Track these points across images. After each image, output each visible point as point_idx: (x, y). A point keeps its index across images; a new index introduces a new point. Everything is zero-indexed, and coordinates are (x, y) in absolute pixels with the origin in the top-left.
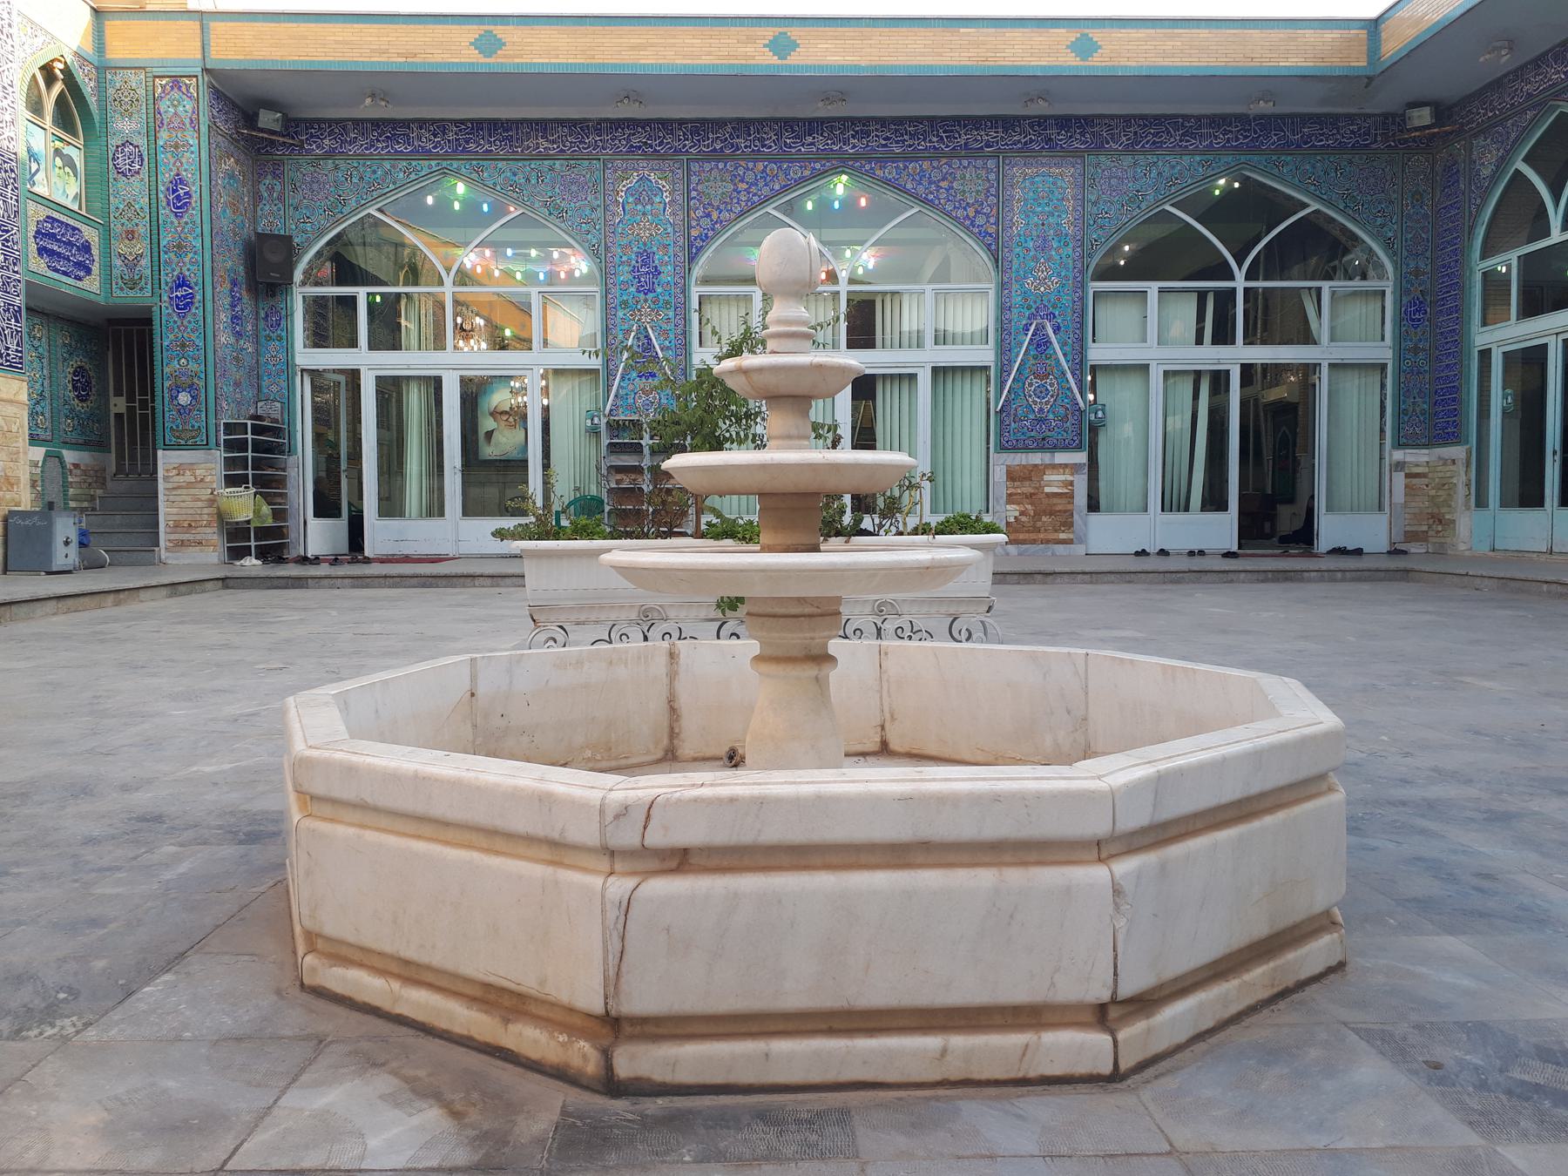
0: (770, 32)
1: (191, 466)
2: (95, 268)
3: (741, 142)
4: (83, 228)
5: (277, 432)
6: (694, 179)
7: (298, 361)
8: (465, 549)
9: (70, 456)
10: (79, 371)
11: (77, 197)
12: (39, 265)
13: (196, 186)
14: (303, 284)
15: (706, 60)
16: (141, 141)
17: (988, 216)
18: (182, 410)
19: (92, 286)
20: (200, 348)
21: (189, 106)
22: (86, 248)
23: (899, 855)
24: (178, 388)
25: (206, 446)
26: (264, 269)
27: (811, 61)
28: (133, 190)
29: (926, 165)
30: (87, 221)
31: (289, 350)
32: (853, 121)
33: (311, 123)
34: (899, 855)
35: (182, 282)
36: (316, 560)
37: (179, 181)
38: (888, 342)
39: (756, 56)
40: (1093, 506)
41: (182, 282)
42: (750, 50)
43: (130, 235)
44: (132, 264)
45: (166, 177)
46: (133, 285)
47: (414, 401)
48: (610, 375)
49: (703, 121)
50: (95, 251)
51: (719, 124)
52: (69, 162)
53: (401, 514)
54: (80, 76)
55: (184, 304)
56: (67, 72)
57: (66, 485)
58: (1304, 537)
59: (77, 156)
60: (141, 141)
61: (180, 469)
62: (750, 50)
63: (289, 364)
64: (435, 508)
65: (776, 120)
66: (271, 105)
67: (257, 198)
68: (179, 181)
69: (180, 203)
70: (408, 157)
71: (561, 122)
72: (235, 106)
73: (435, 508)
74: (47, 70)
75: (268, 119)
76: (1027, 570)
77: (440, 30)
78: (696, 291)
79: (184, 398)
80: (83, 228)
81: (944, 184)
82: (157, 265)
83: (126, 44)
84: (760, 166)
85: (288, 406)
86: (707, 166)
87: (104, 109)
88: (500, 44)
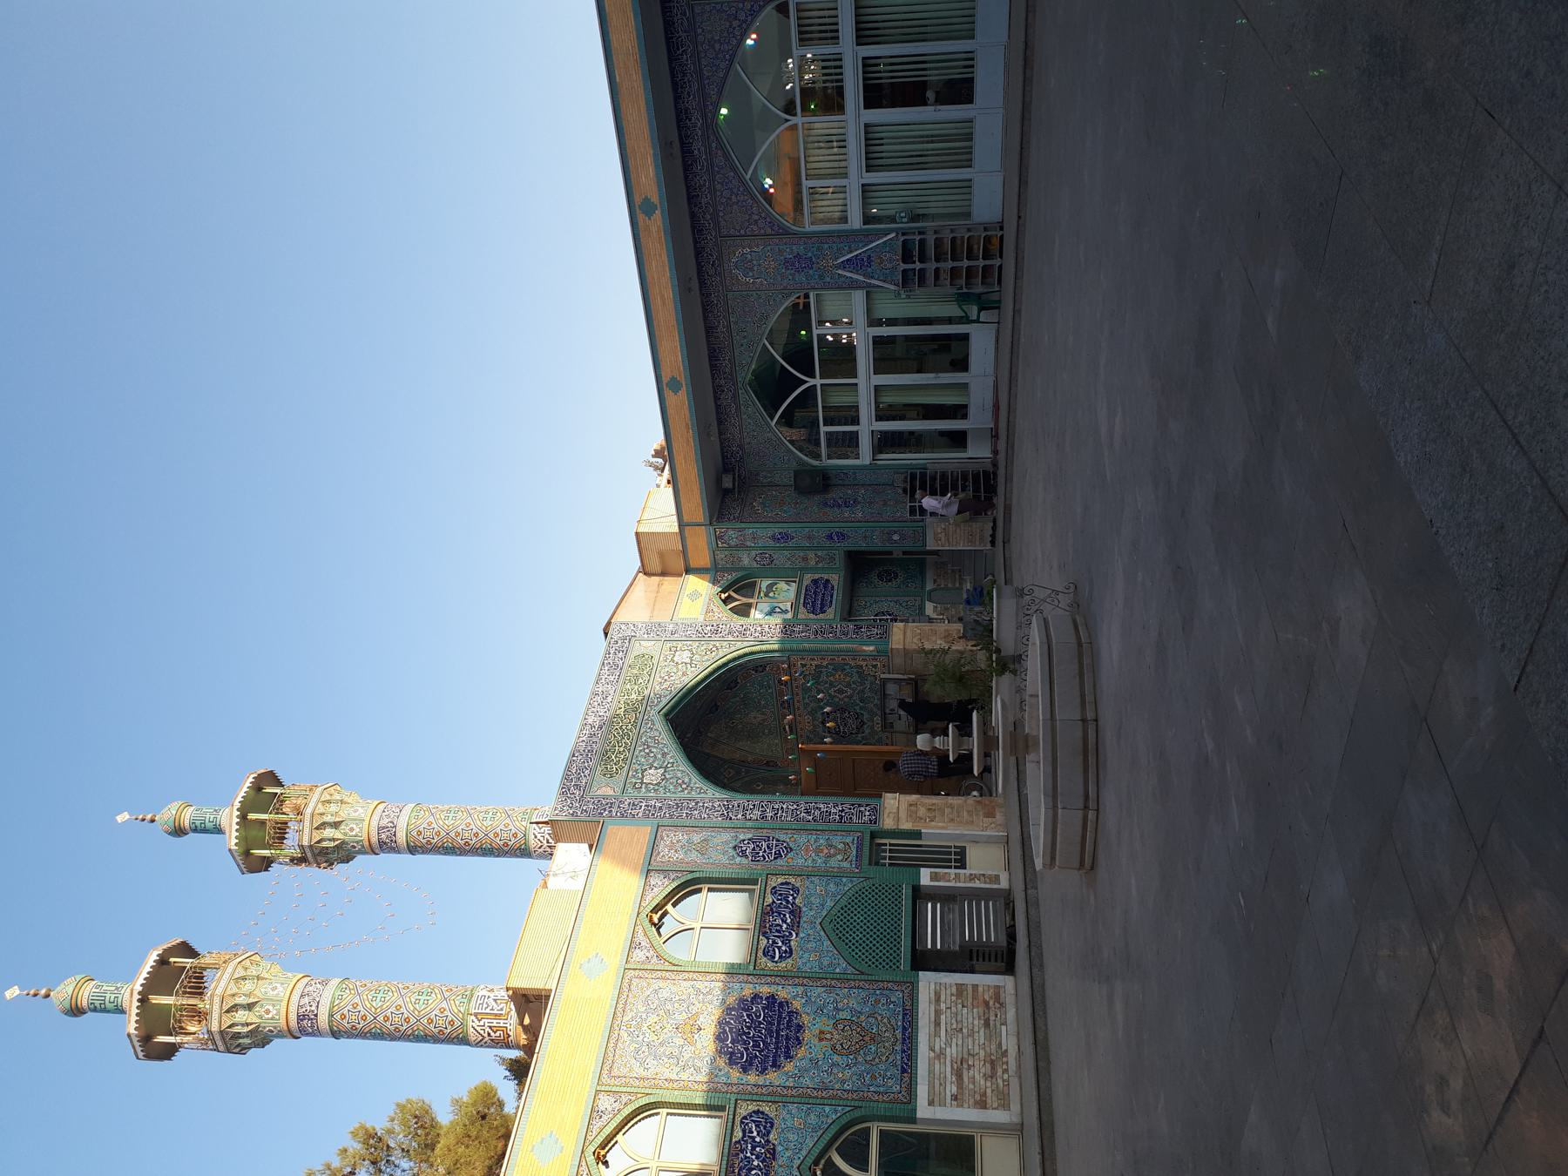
0: (641, 217)
1: (935, 534)
2: (826, 577)
3: (704, 201)
4: (805, 584)
5: (913, 476)
6: (732, 232)
7: (867, 462)
8: (990, 370)
9: (929, 586)
10: (880, 577)
11: (787, 582)
12: (830, 613)
13: (776, 529)
14: (817, 456)
15: (665, 258)
16: (753, 553)
17: (738, 9)
18: (903, 537)
19: (836, 579)
20: (867, 528)
21: (731, 532)
22: (815, 582)
23: (1051, 682)
24: (890, 539)
25: (924, 528)
26: (816, 484)
27: (655, 188)
28: (781, 558)
29: (704, 62)
30: (801, 582)
31: (863, 468)
32: (679, 121)
33: (723, 457)
34: (1051, 682)
35: (830, 537)
36: (995, 452)
37: (773, 537)
38: (832, 13)
39: (657, 223)
40: (968, 215)
41: (830, 537)
42: (654, 229)
43: (805, 559)
44: (820, 559)
45: (772, 543)
46: (832, 559)
47: (888, 399)
48: (870, 285)
49: (693, 228)
50: (817, 576)
51: (693, 215)
52: (770, 587)
53: (966, 406)
54: (725, 582)
55: (842, 536)
56: (723, 592)
57: (946, 588)
58: (990, 244)
59: (765, 583)
60: (753, 553)
61: (937, 539)
62: (654, 229)
63: (871, 468)
64: (964, 387)
65: (686, 177)
66: (719, 481)
67: (771, 485)
68: (773, 537)
69: (785, 537)
70: (738, 409)
71: (705, 318)
72: (723, 501)
73: (964, 387)
74: (725, 601)
75: (727, 482)
76: (1021, 63)
77: (670, 411)
78: (809, 228)
79: (896, 537)
80: (805, 584)
81: (717, 46)
82: (822, 548)
83: (702, 557)
84: (718, 187)
85: (896, 469)
86: (723, 223)
87: (737, 570)
88: (673, 379)
